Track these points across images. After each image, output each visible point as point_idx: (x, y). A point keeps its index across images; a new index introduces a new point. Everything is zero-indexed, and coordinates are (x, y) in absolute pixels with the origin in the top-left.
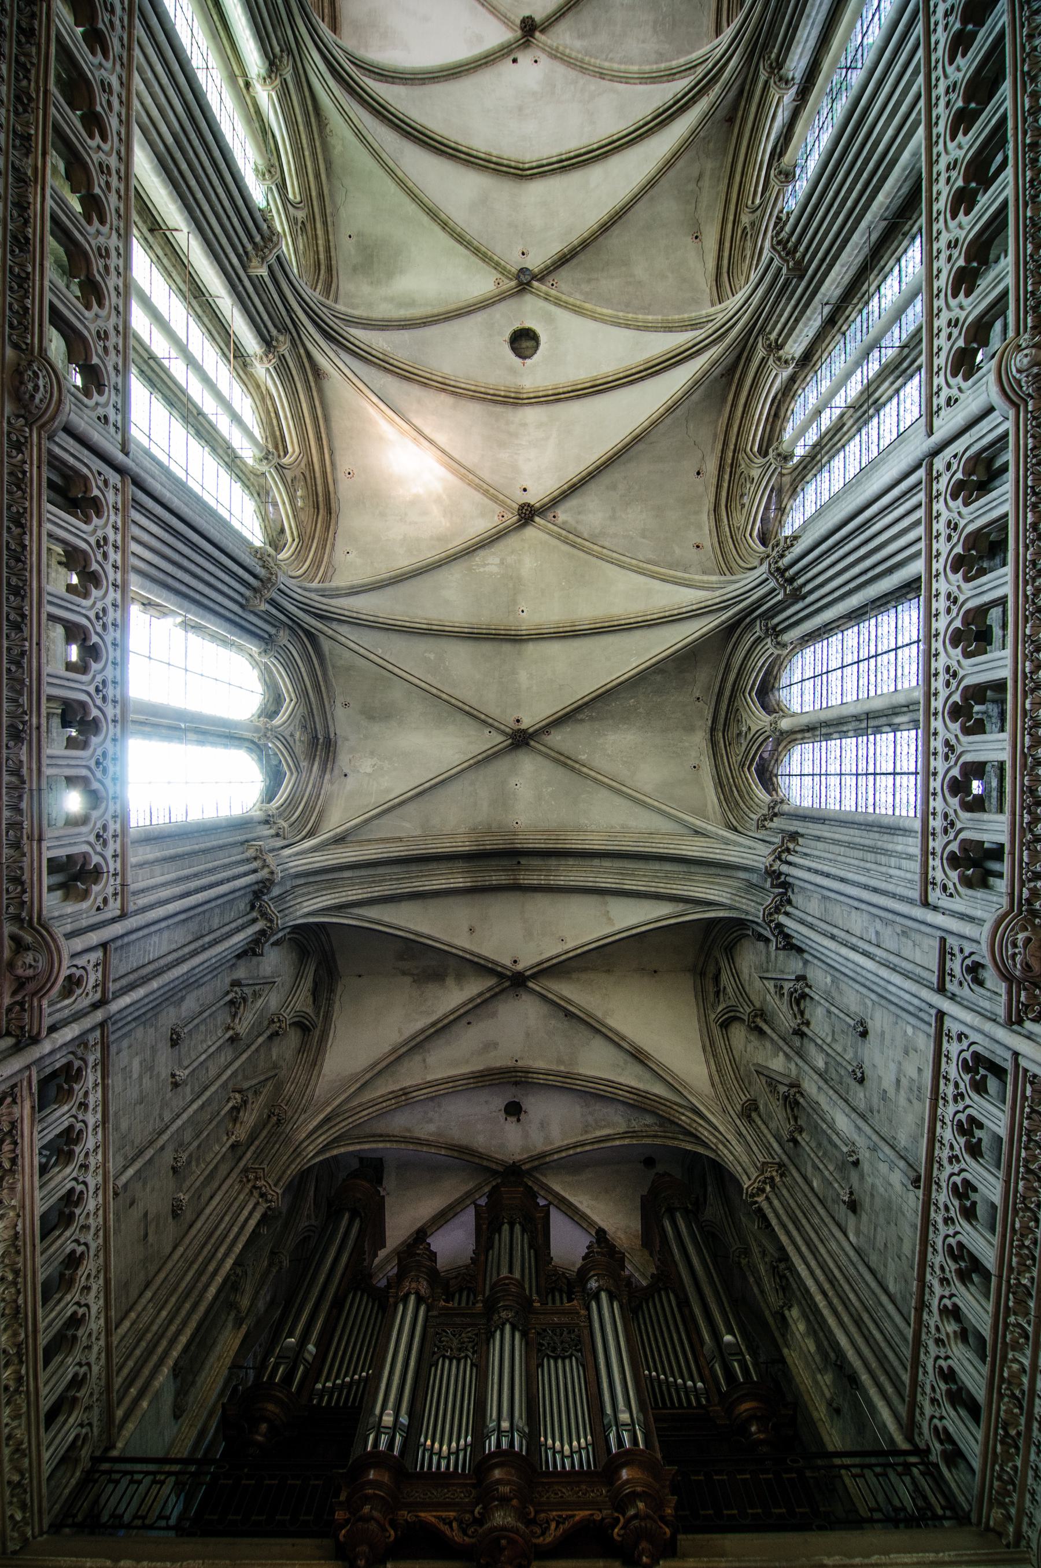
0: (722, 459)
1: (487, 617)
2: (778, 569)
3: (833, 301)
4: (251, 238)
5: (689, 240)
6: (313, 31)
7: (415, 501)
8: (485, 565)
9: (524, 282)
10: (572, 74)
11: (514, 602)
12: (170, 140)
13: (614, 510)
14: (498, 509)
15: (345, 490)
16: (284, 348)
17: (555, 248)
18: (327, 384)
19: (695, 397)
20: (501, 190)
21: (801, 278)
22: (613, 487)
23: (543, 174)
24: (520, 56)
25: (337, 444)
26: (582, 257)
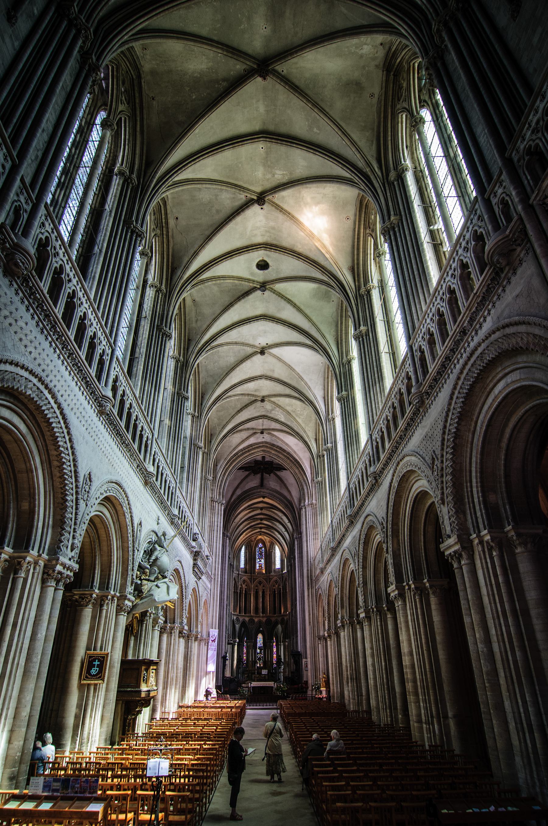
0: (167, 228)
1: (282, 149)
2: (140, 236)
3: (143, 319)
4: (363, 340)
5: (197, 299)
6: (334, 369)
7: (318, 203)
8: (283, 174)
9: (263, 286)
10: (247, 342)
11: (267, 153)
12: (378, 385)
13: (216, 199)
14: (276, 200)
15: (351, 211)
16: (363, 289)
17: (251, 297)
18: (350, 264)
19: (186, 259)
20: (272, 311)
21: (157, 326)
22: (218, 211)
23: (256, 317)
24: (265, 345)
25: (350, 233)
26: (240, 294)
